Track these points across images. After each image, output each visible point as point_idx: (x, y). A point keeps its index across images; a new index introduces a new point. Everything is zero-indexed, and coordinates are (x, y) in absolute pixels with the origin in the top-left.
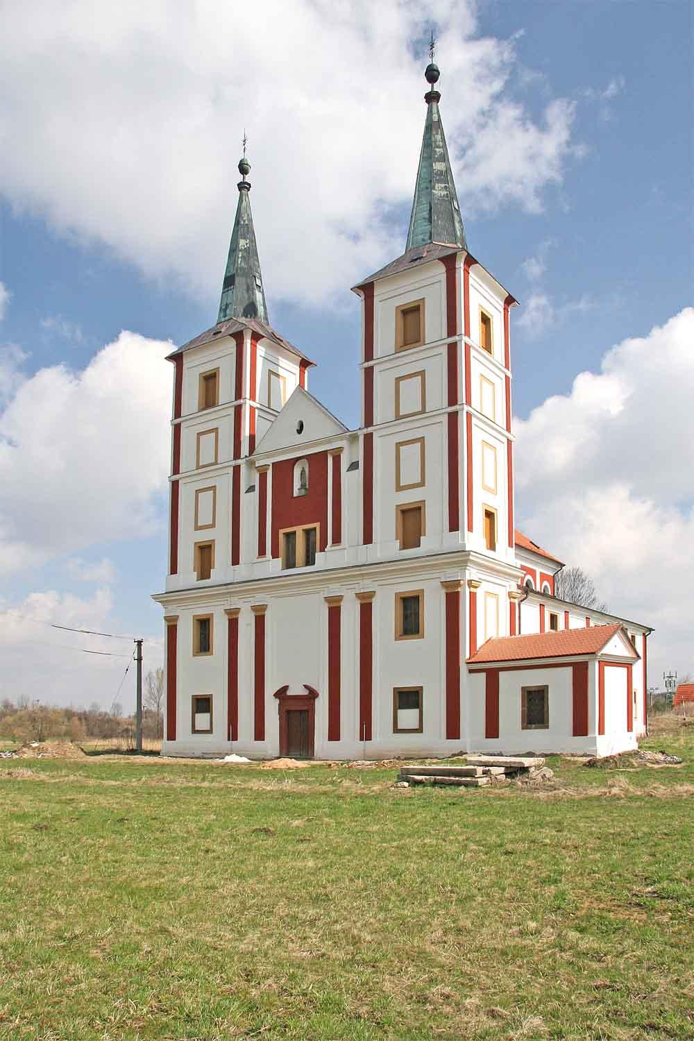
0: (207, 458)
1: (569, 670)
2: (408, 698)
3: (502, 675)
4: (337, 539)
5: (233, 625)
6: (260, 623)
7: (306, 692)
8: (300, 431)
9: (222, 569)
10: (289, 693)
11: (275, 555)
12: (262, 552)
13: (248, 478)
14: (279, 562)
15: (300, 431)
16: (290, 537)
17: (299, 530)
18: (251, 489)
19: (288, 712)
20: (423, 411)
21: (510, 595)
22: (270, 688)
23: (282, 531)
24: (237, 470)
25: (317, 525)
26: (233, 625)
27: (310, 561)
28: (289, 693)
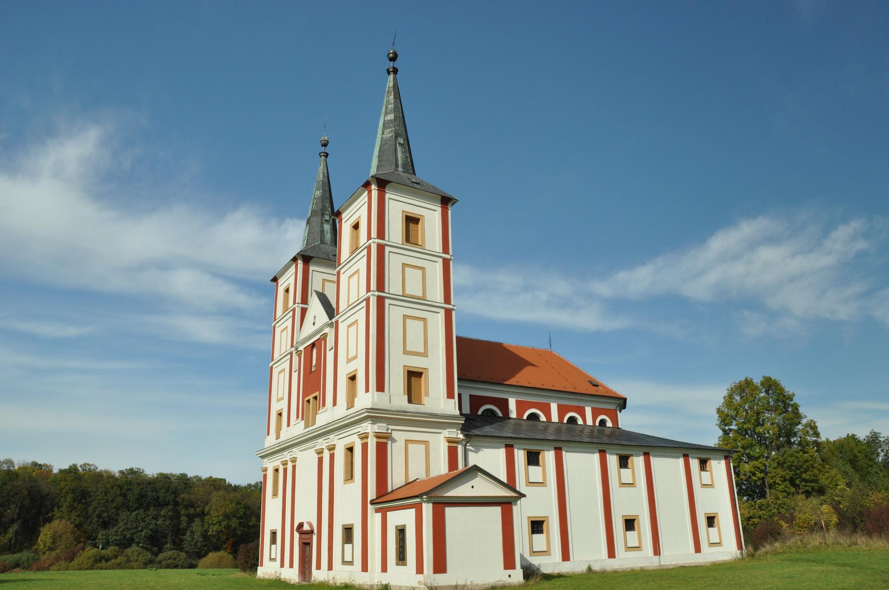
4: (324, 405)
12: (298, 417)
16: (308, 401)
17: (311, 397)
25: (317, 394)
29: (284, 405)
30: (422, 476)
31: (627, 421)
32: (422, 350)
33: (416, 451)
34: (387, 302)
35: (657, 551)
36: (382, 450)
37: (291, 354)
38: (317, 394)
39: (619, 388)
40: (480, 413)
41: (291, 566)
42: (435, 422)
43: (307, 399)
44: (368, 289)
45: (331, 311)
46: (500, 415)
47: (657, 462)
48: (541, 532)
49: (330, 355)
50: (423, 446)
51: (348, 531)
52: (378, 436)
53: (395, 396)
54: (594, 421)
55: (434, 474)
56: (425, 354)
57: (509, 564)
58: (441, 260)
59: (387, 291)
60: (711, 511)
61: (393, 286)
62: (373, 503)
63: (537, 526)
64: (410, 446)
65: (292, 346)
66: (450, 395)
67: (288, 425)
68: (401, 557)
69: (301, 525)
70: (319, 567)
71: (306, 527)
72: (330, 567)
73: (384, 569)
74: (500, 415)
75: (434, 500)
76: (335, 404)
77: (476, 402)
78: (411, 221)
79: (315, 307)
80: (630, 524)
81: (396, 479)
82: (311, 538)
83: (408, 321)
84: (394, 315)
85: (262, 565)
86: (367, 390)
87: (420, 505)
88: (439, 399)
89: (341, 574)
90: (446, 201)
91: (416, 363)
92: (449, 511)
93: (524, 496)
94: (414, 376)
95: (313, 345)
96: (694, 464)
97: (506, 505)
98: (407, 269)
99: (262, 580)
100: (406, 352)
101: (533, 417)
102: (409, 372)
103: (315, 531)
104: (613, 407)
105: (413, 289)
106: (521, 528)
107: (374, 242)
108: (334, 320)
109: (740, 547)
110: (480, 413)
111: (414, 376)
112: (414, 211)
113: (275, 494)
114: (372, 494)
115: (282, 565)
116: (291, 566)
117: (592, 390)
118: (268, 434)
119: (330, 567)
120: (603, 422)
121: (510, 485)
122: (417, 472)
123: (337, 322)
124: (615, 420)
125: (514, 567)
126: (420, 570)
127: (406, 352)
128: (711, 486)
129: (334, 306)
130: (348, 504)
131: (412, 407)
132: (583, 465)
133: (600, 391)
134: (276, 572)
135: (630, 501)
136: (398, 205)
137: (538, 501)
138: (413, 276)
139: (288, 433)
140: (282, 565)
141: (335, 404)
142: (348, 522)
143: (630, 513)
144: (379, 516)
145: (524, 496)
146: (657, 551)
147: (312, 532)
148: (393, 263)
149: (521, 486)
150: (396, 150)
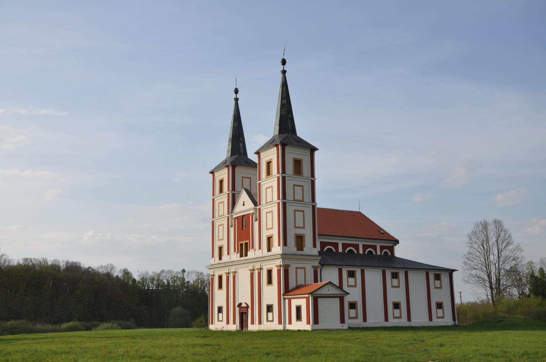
0: (221, 214)
1: (305, 299)
2: (270, 308)
4: (253, 248)
5: (228, 278)
6: (234, 277)
7: (245, 305)
8: (244, 205)
9: (225, 258)
10: (242, 306)
11: (238, 253)
12: (235, 251)
13: (232, 222)
14: (239, 254)
15: (244, 205)
16: (242, 245)
17: (244, 242)
20: (272, 201)
21: (313, 267)
22: (237, 304)
24: (228, 218)
25: (247, 241)
26: (228, 278)
27: (246, 255)
28: (242, 306)
29: (224, 244)
30: (303, 284)
32: (302, 226)
33: (301, 272)
34: (287, 204)
35: (409, 319)
38: (247, 241)
40: (325, 250)
43: (240, 243)
46: (334, 251)
47: (412, 276)
49: (256, 224)
50: (303, 270)
56: (304, 228)
58: (310, 181)
59: (287, 199)
60: (439, 300)
61: (289, 196)
64: (298, 270)
66: (315, 246)
70: (253, 323)
71: (244, 305)
72: (260, 323)
74: (334, 251)
75: (315, 295)
77: (323, 245)
79: (244, 197)
81: (292, 285)
83: (296, 212)
85: (212, 323)
88: (310, 249)
89: (266, 326)
91: (300, 232)
92: (319, 300)
95: (244, 216)
99: (211, 331)
100: (295, 227)
101: (351, 251)
102: (297, 236)
104: (391, 245)
105: (299, 197)
108: (258, 207)
109: (454, 319)
110: (325, 250)
112: (298, 157)
113: (220, 287)
115: (228, 323)
116: (234, 323)
118: (213, 257)
119: (260, 323)
120: (386, 252)
121: (341, 287)
126: (308, 323)
127: (295, 227)
128: (441, 288)
131: (299, 252)
132: (373, 277)
134: (223, 327)
135: (396, 295)
137: (354, 295)
138: (298, 190)
140: (228, 323)
142: (270, 303)
143: (397, 300)
146: (409, 319)
147: (248, 307)
149: (345, 288)
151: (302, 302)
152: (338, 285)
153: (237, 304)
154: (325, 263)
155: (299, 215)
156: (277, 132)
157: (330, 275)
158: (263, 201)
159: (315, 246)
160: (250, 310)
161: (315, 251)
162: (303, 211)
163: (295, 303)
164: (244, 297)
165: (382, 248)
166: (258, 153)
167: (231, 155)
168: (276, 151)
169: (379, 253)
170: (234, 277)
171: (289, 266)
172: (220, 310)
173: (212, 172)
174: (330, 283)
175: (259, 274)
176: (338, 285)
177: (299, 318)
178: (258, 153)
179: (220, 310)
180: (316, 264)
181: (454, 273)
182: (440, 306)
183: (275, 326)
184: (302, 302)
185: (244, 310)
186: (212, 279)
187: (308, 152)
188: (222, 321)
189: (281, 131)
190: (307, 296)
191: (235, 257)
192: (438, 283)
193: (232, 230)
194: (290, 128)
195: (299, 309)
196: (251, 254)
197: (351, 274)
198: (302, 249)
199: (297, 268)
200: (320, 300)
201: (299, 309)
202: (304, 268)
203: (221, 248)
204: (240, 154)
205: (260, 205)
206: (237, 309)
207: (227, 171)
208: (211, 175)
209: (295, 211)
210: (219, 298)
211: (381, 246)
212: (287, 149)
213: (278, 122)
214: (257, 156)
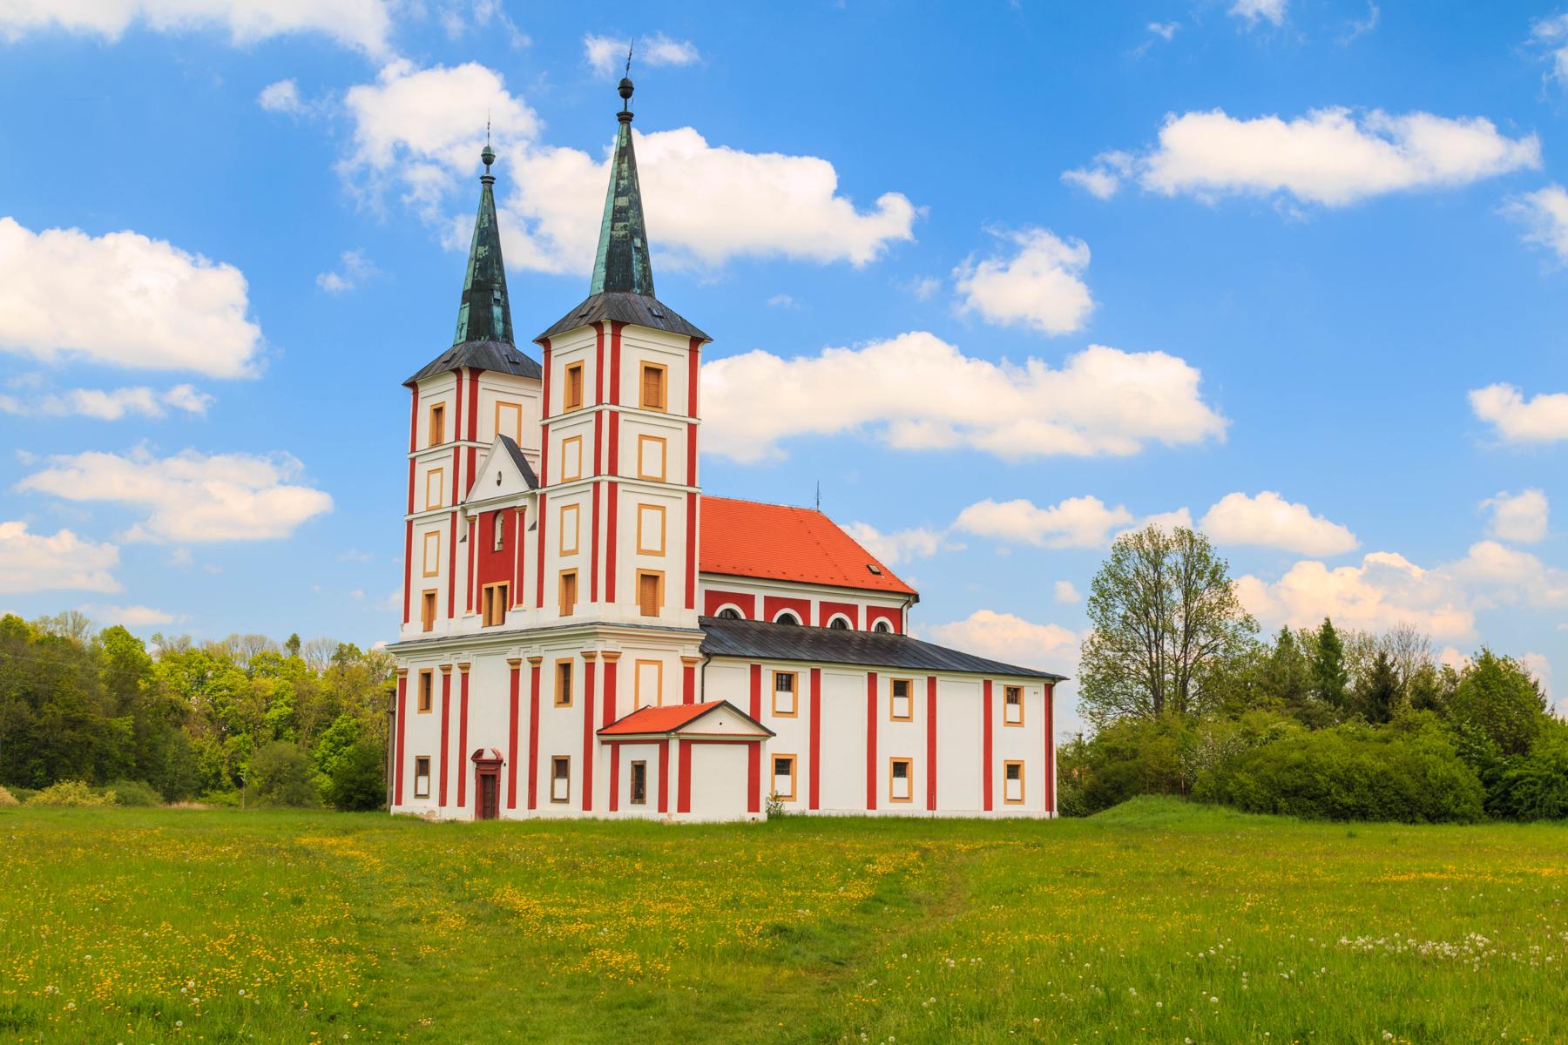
2: (561, 767)
3: (622, 747)
4: (520, 601)
5: (447, 679)
6: (465, 677)
7: (493, 757)
8: (499, 483)
11: (479, 611)
12: (469, 607)
13: (462, 528)
15: (499, 483)
16: (490, 590)
17: (495, 585)
18: (464, 540)
19: (484, 777)
21: (684, 660)
22: (470, 753)
23: (485, 586)
25: (507, 583)
26: (447, 679)
30: (654, 704)
31: (918, 627)
33: (649, 672)
34: (620, 488)
35: (931, 804)
36: (610, 670)
37: (454, 514)
38: (507, 583)
39: (912, 583)
40: (717, 614)
41: (461, 803)
42: (671, 635)
44: (597, 472)
45: (531, 480)
48: (787, 773)
49: (531, 539)
51: (561, 767)
52: (606, 655)
53: (626, 608)
54: (869, 626)
55: (666, 703)
56: (662, 553)
57: (753, 805)
60: (1014, 757)
61: (627, 467)
62: (600, 733)
63: (783, 766)
64: (642, 667)
65: (455, 503)
66: (690, 604)
67: (451, 615)
68: (638, 795)
69: (479, 753)
72: (532, 804)
73: (614, 806)
74: (743, 616)
76: (540, 604)
77: (713, 599)
78: (653, 373)
80: (900, 769)
81: (623, 708)
82: (498, 769)
84: (627, 503)
85: (399, 802)
86: (594, 598)
87: (667, 742)
88: (677, 613)
90: (697, 340)
91: (651, 564)
92: (695, 748)
93: (772, 734)
94: (650, 580)
95: (498, 512)
96: (999, 695)
97: (754, 747)
98: (645, 442)
103: (506, 760)
104: (897, 605)
105: (652, 469)
106: (767, 766)
107: (607, 408)
108: (538, 492)
109: (1049, 807)
110: (717, 614)
111: (650, 580)
112: (655, 359)
113: (426, 705)
114: (598, 723)
115: (443, 802)
116: (461, 803)
117: (870, 581)
118: (407, 620)
119: (532, 804)
120: (882, 626)
122: (648, 699)
123: (543, 496)
124: (899, 625)
125: (757, 810)
126: (663, 807)
127: (640, 551)
128: (1020, 724)
129: (536, 468)
130: (562, 730)
132: (844, 690)
133: (882, 582)
136: (638, 349)
137: (789, 738)
138: (652, 449)
139: (443, 627)
140: (443, 802)
141: (540, 604)
142: (561, 753)
143: (901, 755)
144: (608, 748)
145: (772, 734)
148: (628, 433)
149: (766, 719)
150: (631, 259)
151: (650, 754)
152: (748, 713)
153: (470, 753)
154: (716, 650)
155: (651, 519)
156: (600, 286)
157: (727, 682)
158: (553, 478)
159: (690, 604)
160: (505, 772)
161: (691, 619)
162: (662, 508)
163: (629, 754)
164: (489, 735)
165: (873, 612)
166: (544, 341)
167: (469, 339)
168: (595, 341)
169: (862, 626)
170: (465, 677)
171: (616, 655)
172: (423, 766)
173: (412, 385)
174: (724, 704)
175: (536, 673)
176: (748, 713)
177: (638, 795)
178: (544, 341)
179: (423, 766)
180: (693, 652)
181: (1059, 687)
182: (1013, 771)
183: (574, 811)
184: (650, 754)
185: (489, 771)
186: (403, 682)
187: (683, 347)
188: (426, 796)
189: (609, 285)
190: (664, 736)
191: (473, 624)
192: (1013, 710)
193: (462, 549)
194: (637, 276)
195: (639, 769)
196: (517, 620)
197: (785, 683)
198: (655, 613)
199: (639, 662)
200: (696, 750)
201: (639, 769)
202: (659, 663)
203: (430, 597)
204: (493, 338)
205: (544, 485)
206: (471, 767)
207: (454, 385)
208: (410, 391)
209: (641, 506)
210: (421, 734)
211: (869, 609)
212: (624, 332)
213: (603, 259)
214: (541, 348)
